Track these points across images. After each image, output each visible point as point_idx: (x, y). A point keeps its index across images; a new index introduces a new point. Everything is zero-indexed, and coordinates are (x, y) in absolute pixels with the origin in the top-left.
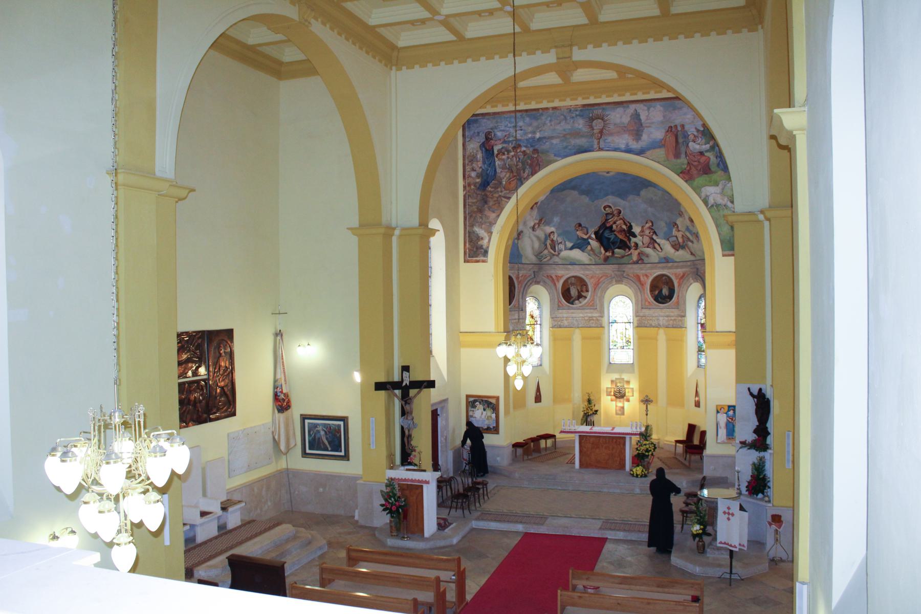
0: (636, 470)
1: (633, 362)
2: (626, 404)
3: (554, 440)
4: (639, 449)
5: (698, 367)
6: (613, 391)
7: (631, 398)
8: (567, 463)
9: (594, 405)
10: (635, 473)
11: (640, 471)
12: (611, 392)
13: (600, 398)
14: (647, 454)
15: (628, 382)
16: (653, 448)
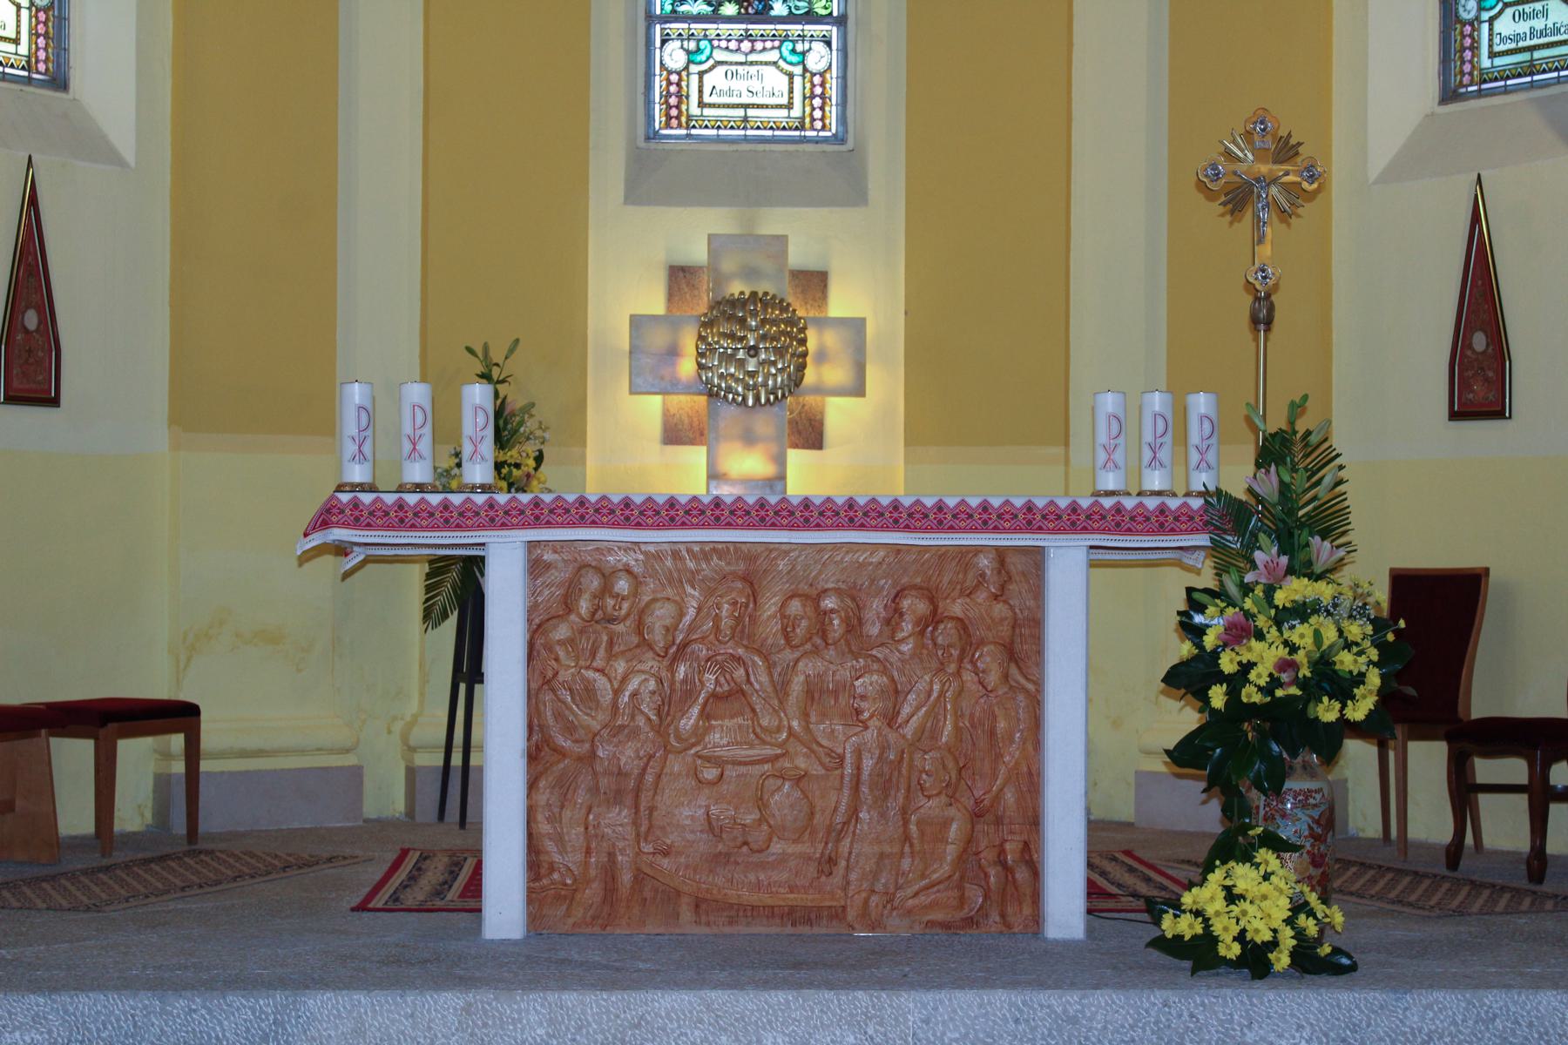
0: (1232, 897)
1: (843, 119)
2: (798, 461)
3: (177, 741)
4: (1227, 664)
5: (1449, 94)
6: (689, 343)
7: (838, 413)
8: (362, 907)
9: (539, 459)
10: (1225, 929)
11: (1279, 909)
12: (673, 352)
13: (579, 407)
14: (1327, 711)
15: (815, 282)
16: (1374, 654)
